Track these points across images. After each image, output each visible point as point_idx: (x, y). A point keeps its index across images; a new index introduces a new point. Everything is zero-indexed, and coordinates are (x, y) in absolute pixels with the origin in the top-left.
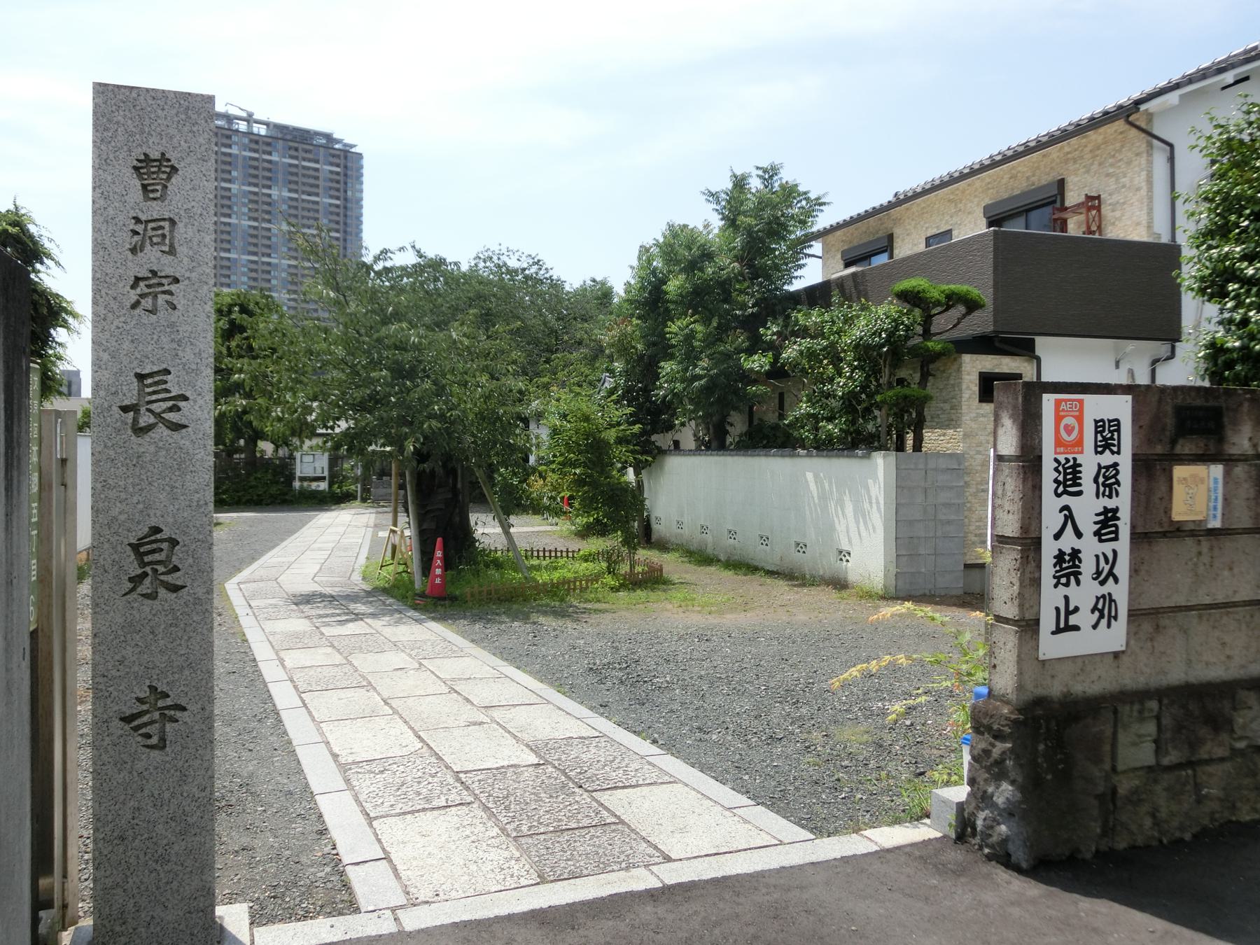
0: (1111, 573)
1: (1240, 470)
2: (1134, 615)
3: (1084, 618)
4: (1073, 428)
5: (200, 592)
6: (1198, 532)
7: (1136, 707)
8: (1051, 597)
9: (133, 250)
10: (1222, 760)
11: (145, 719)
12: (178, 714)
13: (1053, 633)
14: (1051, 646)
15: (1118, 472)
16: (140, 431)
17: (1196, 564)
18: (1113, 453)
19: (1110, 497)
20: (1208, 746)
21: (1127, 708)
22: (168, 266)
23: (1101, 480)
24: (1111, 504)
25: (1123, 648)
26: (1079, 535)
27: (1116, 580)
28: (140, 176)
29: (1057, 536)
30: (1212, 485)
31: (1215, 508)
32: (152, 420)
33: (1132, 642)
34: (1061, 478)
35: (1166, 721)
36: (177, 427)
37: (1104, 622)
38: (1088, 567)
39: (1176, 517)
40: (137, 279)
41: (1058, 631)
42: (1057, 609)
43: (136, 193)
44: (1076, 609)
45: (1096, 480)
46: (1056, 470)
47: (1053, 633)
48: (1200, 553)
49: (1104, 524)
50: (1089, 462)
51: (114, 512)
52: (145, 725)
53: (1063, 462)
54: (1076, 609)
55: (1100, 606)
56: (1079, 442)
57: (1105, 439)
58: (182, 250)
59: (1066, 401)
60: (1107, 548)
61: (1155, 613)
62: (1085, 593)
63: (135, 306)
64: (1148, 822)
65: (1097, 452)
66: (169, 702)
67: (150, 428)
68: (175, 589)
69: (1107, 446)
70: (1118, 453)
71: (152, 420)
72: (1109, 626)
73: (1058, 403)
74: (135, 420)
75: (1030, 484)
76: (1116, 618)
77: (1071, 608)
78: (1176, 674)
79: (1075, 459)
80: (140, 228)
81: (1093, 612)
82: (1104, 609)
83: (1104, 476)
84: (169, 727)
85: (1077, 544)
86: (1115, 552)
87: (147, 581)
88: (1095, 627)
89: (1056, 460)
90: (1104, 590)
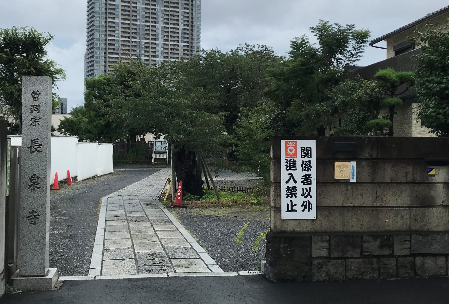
0: (309, 194)
1: (364, 163)
2: (318, 208)
3: (299, 208)
4: (293, 150)
5: (44, 189)
6: (346, 182)
7: (319, 237)
8: (285, 201)
9: (31, 112)
10: (357, 258)
11: (31, 217)
12: (39, 217)
13: (286, 211)
14: (285, 215)
15: (311, 163)
16: (32, 152)
17: (346, 194)
18: (308, 157)
19: (308, 171)
20: (350, 253)
21: (316, 237)
22: (38, 115)
23: (304, 166)
24: (308, 173)
25: (315, 218)
26: (295, 182)
27: (311, 197)
28: (32, 96)
29: (287, 182)
30: (351, 168)
31: (353, 175)
32: (34, 150)
33: (319, 217)
34: (288, 165)
35: (333, 242)
36: (39, 151)
37: (307, 210)
38: (299, 192)
39: (336, 178)
40: (32, 119)
41: (288, 211)
42: (288, 205)
43: (31, 100)
44: (295, 205)
45: (302, 166)
46: (286, 162)
47: (286, 211)
48: (348, 190)
49: (305, 179)
50: (299, 161)
51: (26, 171)
52: (31, 219)
53: (289, 160)
54: (295, 205)
55: (305, 204)
56: (295, 154)
57: (305, 153)
58: (41, 112)
59: (290, 142)
60: (307, 187)
61: (329, 208)
62: (299, 200)
63: (31, 125)
64: (324, 274)
65: (302, 157)
66: (36, 214)
67: (34, 152)
68: (38, 188)
69: (306, 155)
70: (311, 157)
71: (34, 150)
72: (309, 211)
73: (286, 143)
74: (31, 150)
75: (277, 166)
76: (311, 209)
77: (293, 204)
78: (339, 228)
79: (293, 159)
80: (32, 107)
81: (302, 206)
82: (307, 206)
83: (305, 164)
84: (36, 219)
85: (295, 185)
86: (310, 188)
87: (33, 186)
88: (303, 211)
89: (286, 159)
90: (307, 199)
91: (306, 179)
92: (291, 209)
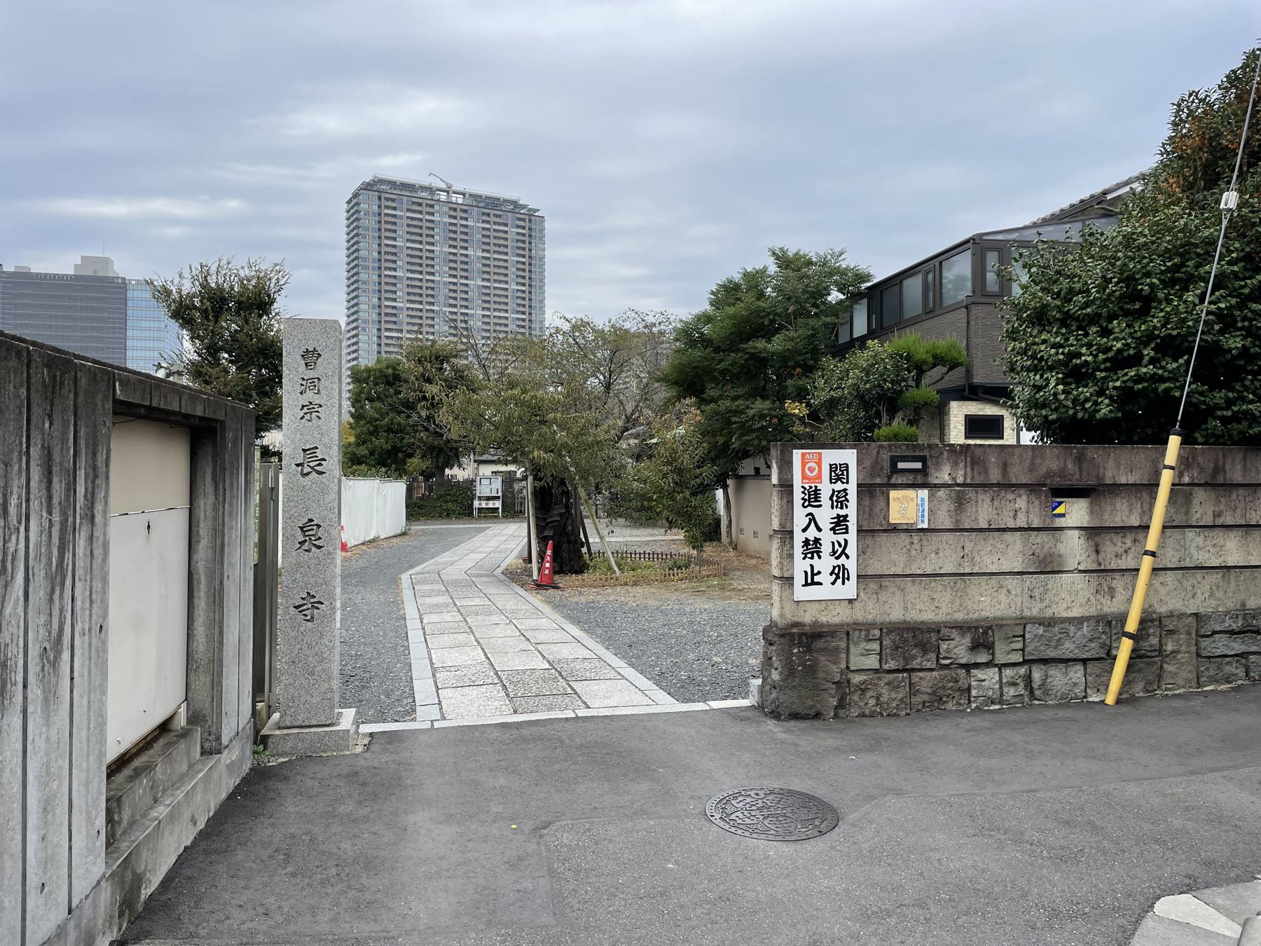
0: (843, 552)
1: (942, 493)
3: (825, 578)
5: (331, 549)
6: (909, 530)
8: (801, 566)
10: (931, 670)
20: (919, 660)
22: (317, 400)
24: (842, 512)
26: (819, 530)
27: (848, 557)
29: (804, 530)
35: (886, 642)
37: (840, 581)
38: (826, 548)
39: (892, 521)
41: (806, 584)
42: (806, 572)
43: (303, 367)
44: (819, 573)
45: (831, 498)
49: (838, 524)
50: (826, 489)
54: (819, 573)
56: (819, 477)
60: (841, 538)
62: (825, 564)
64: (872, 702)
67: (308, 474)
68: (320, 547)
69: (839, 479)
73: (803, 455)
78: (896, 614)
82: (840, 574)
84: (316, 611)
85: (818, 535)
86: (846, 541)
88: (833, 583)
90: (840, 562)
91: (840, 524)
92: (811, 581)
